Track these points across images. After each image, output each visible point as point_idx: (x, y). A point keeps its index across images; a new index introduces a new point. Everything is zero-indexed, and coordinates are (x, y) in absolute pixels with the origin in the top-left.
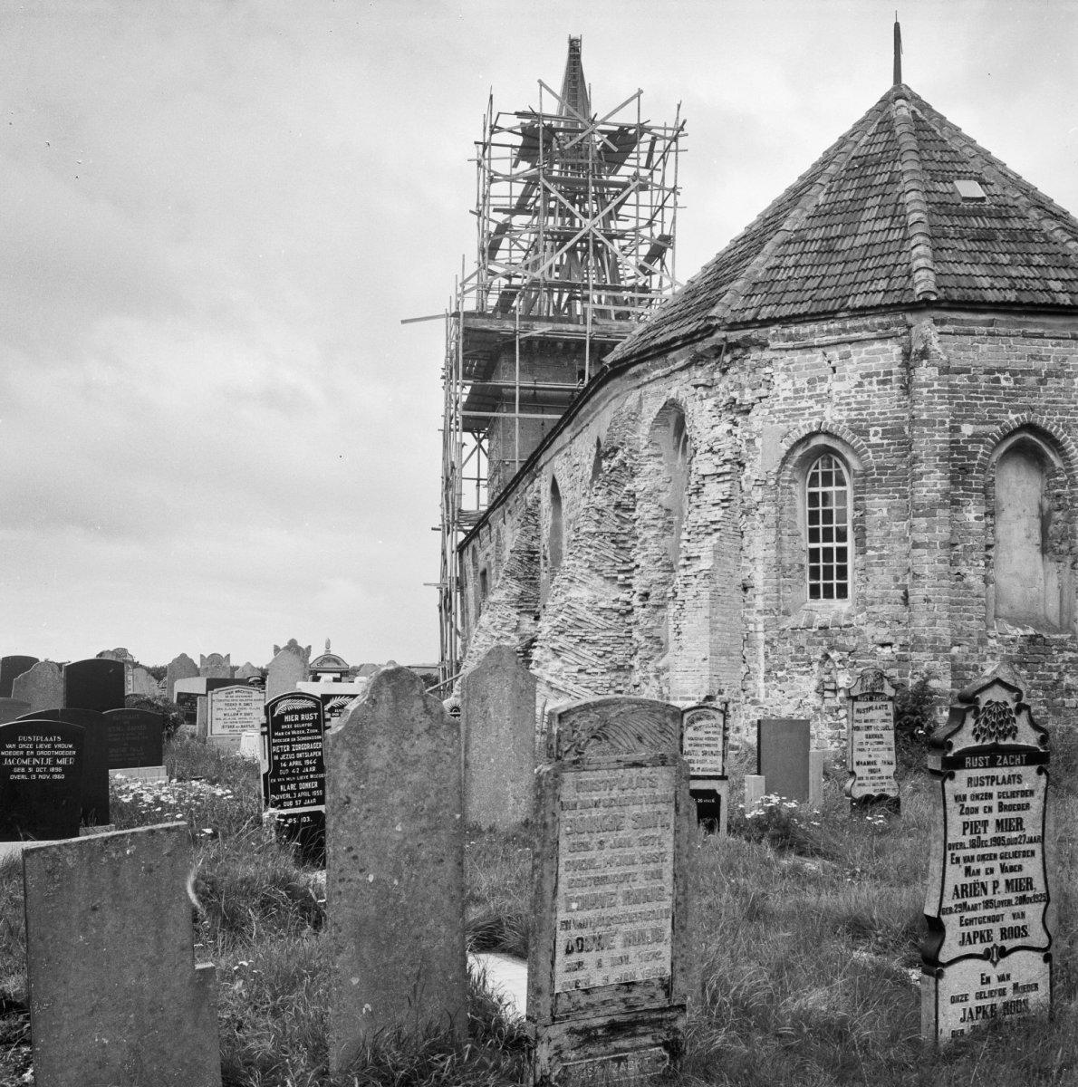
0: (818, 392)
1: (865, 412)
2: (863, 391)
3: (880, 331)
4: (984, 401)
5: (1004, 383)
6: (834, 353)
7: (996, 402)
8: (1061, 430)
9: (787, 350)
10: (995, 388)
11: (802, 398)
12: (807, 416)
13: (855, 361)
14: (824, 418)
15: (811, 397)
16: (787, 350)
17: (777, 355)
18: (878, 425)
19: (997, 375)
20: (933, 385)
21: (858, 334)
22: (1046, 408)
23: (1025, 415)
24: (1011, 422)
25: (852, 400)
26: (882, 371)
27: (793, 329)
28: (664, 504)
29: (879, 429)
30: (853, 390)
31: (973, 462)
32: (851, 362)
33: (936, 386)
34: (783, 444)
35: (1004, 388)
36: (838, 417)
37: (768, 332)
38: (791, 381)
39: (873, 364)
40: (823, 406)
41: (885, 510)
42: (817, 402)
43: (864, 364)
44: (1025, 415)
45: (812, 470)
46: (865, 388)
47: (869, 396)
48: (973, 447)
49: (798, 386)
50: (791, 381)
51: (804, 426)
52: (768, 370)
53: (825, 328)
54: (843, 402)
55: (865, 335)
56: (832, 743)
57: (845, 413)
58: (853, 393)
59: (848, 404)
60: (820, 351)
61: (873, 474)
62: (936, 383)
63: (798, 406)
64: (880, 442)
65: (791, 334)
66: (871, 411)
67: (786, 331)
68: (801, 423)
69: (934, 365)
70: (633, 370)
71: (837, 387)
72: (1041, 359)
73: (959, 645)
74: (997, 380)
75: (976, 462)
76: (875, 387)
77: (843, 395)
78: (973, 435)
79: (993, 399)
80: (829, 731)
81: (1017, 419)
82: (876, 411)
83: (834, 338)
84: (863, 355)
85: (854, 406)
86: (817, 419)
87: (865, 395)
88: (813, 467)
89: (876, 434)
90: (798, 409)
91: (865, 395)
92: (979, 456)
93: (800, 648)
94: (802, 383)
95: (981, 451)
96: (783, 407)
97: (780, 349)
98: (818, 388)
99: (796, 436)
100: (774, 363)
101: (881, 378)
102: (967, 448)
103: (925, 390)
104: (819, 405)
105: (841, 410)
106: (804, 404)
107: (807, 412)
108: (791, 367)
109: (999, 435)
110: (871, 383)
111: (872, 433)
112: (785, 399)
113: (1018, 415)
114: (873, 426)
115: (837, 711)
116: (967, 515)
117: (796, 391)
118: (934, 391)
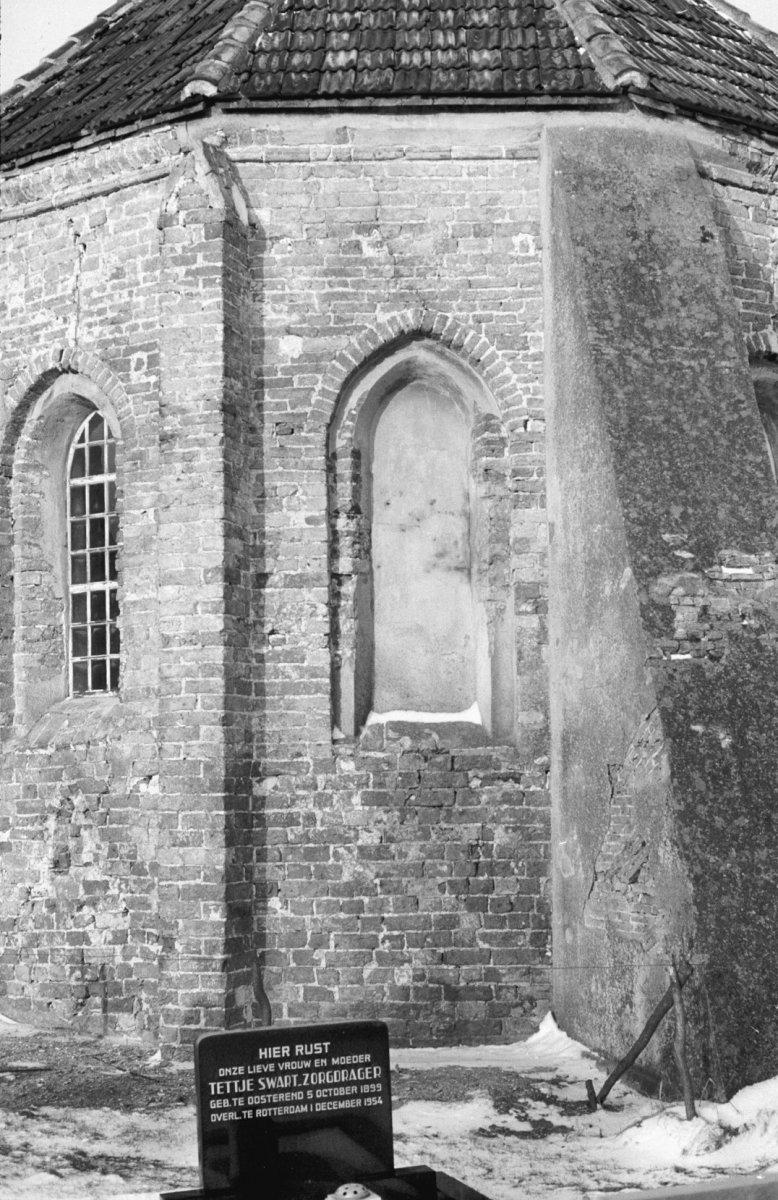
0: (59, 294)
1: (123, 326)
2: (122, 287)
3: (146, 166)
4: (327, 289)
5: (368, 252)
6: (84, 216)
7: (350, 290)
8: (484, 339)
10: (349, 262)
11: (36, 307)
12: (42, 341)
13: (111, 231)
14: (66, 343)
15: (49, 305)
18: (141, 348)
19: (354, 237)
20: (195, 262)
21: (116, 176)
22: (453, 295)
23: (409, 313)
24: (379, 326)
25: (107, 304)
26: (150, 243)
29: (144, 356)
30: (109, 285)
31: (299, 410)
33: (201, 262)
34: (8, 397)
35: (367, 262)
36: (87, 339)
41: (151, 512)
42: (58, 313)
43: (125, 234)
44: (409, 313)
45: (75, 446)
46: (126, 280)
47: (130, 294)
48: (301, 381)
49: (33, 286)
50: (22, 277)
51: (37, 361)
53: (64, 171)
54: (94, 308)
55: (126, 176)
56: (73, 970)
58: (109, 291)
59: (101, 312)
61: (134, 445)
62: (200, 257)
63: (33, 322)
64: (144, 380)
66: (133, 322)
68: (35, 354)
69: (196, 221)
71: (89, 280)
72: (446, 204)
73: (277, 775)
74: (357, 246)
75: (308, 410)
76: (141, 276)
77: (95, 295)
78: (307, 356)
79: (345, 285)
80: (67, 946)
81: (392, 321)
82: (140, 321)
83: (77, 191)
84: (123, 216)
85: (110, 315)
87: (125, 293)
88: (77, 437)
89: (140, 363)
90: (35, 329)
92: (315, 397)
93: (30, 789)
94: (37, 279)
95: (318, 387)
96: (12, 327)
98: (60, 287)
99: (25, 382)
101: (148, 256)
102: (289, 382)
103: (181, 270)
104: (61, 320)
105: (90, 325)
106: (40, 319)
107: (42, 333)
108: (23, 251)
109: (354, 353)
110: (134, 271)
111: (133, 365)
112: (14, 312)
113: (395, 313)
114: (134, 350)
115: (80, 908)
116: (291, 514)
117: (29, 297)
118: (198, 272)
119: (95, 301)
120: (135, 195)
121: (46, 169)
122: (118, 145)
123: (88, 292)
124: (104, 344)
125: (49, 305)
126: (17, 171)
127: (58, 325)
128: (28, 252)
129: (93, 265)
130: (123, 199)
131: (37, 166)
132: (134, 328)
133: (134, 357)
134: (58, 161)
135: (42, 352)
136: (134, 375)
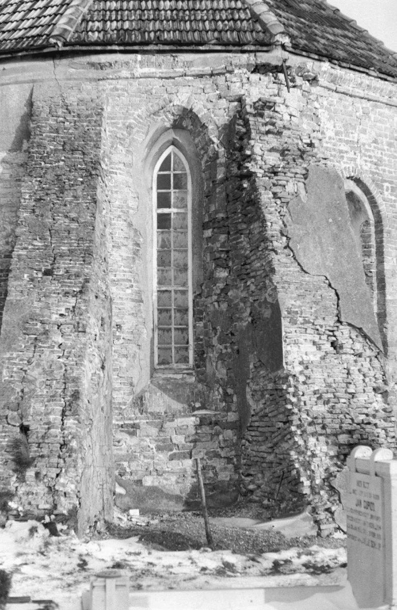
0: (351, 139)
9: (329, 89)
12: (345, 160)
13: (372, 119)
14: (356, 165)
15: (347, 142)
16: (329, 89)
17: (325, 93)
27: (339, 72)
28: (134, 223)
29: (390, 186)
32: (370, 118)
37: (320, 67)
38: (332, 122)
39: (383, 126)
40: (355, 154)
47: (382, 153)
50: (332, 122)
52: (316, 104)
57: (369, 164)
58: (372, 148)
60: (350, 99)
65: (336, 77)
66: (383, 167)
67: (332, 71)
68: (343, 166)
70: (94, 58)
76: (386, 147)
77: (367, 147)
82: (387, 169)
86: (352, 165)
90: (341, 152)
91: (380, 152)
97: (326, 88)
100: (320, 100)
104: (353, 153)
105: (366, 161)
106: (344, 147)
107: (345, 155)
108: (332, 108)
111: (385, 188)
114: (386, 181)
119: (367, 150)
120: (381, 108)
121: (351, 75)
122: (383, 82)
123: (364, 144)
124: (372, 173)
125: (347, 142)
126: (337, 67)
127: (351, 155)
128: (335, 109)
129: (364, 131)
130: (376, 107)
131: (348, 71)
132: (384, 171)
133: (386, 185)
134: (357, 74)
135: (347, 166)
136: (386, 193)
